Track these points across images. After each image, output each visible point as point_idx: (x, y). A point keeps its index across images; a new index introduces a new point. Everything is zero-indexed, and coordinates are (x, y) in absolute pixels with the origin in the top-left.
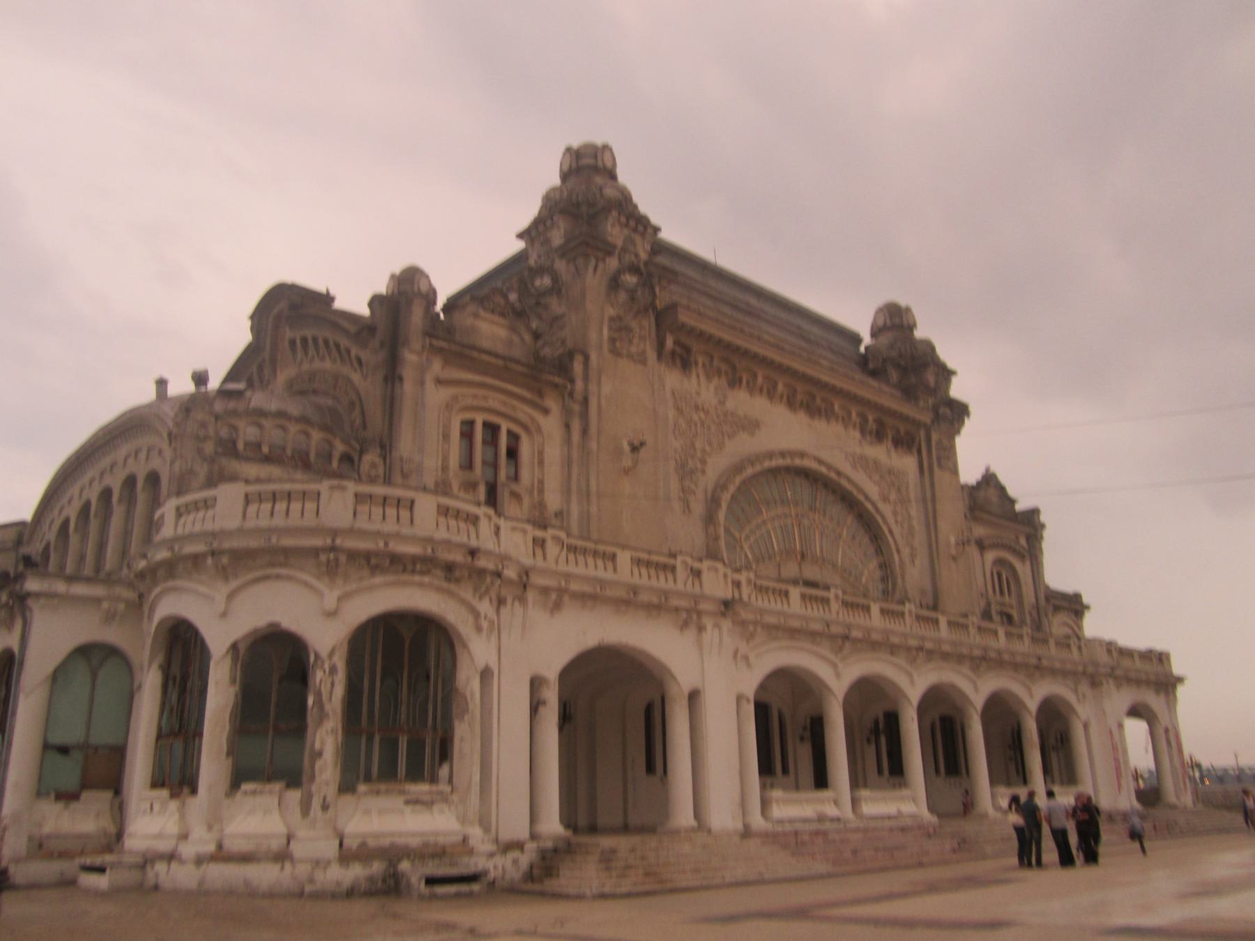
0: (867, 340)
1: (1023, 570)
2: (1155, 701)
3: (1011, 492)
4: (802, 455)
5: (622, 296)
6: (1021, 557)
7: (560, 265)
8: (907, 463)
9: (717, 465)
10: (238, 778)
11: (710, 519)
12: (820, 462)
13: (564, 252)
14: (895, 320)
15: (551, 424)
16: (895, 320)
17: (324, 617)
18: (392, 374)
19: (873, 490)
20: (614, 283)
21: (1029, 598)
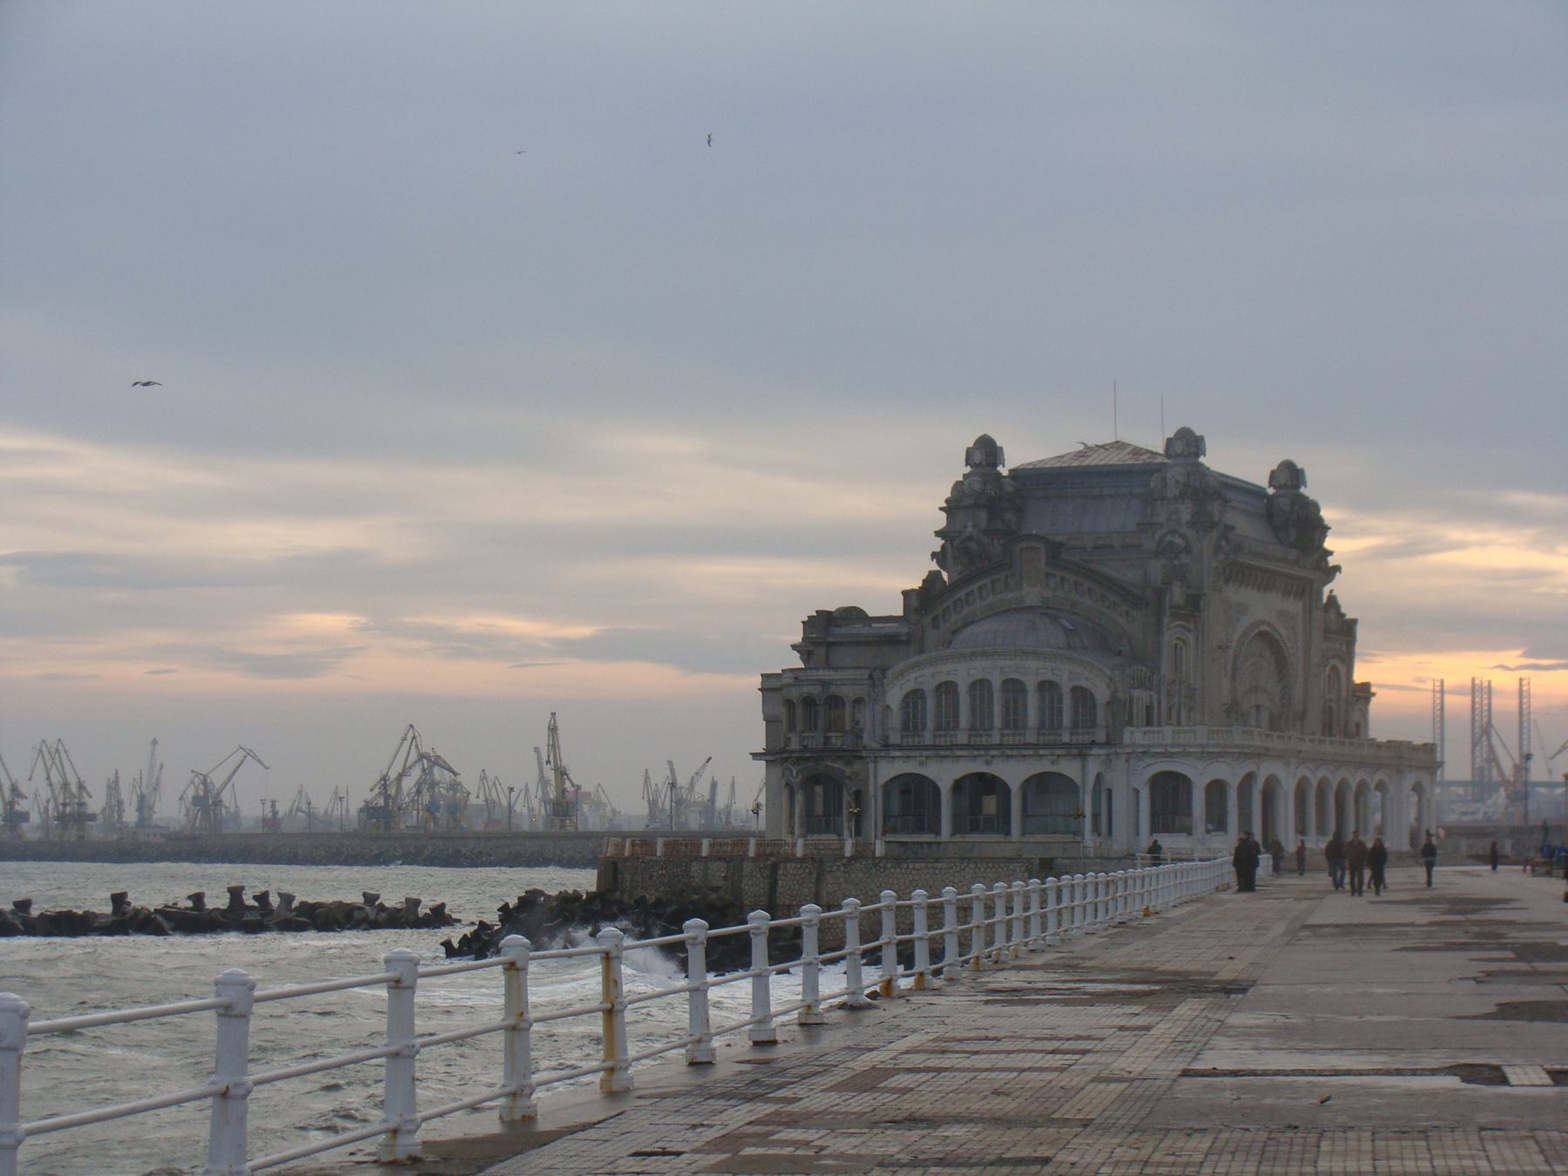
0: (1271, 491)
1: (1342, 670)
2: (1424, 778)
3: (1343, 610)
4: (1263, 623)
5: (1221, 556)
6: (1342, 659)
7: (1190, 533)
8: (1295, 607)
9: (1236, 637)
10: (1208, 831)
11: (1233, 679)
12: (1269, 624)
13: (1192, 524)
14: (1290, 475)
15: (1191, 638)
16: (1290, 475)
17: (1230, 773)
18: (1159, 631)
19: (1284, 632)
20: (1217, 549)
21: (1344, 694)
